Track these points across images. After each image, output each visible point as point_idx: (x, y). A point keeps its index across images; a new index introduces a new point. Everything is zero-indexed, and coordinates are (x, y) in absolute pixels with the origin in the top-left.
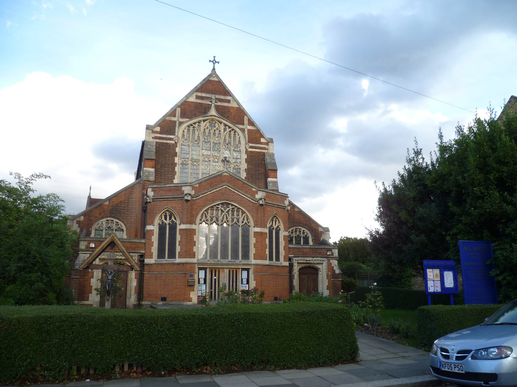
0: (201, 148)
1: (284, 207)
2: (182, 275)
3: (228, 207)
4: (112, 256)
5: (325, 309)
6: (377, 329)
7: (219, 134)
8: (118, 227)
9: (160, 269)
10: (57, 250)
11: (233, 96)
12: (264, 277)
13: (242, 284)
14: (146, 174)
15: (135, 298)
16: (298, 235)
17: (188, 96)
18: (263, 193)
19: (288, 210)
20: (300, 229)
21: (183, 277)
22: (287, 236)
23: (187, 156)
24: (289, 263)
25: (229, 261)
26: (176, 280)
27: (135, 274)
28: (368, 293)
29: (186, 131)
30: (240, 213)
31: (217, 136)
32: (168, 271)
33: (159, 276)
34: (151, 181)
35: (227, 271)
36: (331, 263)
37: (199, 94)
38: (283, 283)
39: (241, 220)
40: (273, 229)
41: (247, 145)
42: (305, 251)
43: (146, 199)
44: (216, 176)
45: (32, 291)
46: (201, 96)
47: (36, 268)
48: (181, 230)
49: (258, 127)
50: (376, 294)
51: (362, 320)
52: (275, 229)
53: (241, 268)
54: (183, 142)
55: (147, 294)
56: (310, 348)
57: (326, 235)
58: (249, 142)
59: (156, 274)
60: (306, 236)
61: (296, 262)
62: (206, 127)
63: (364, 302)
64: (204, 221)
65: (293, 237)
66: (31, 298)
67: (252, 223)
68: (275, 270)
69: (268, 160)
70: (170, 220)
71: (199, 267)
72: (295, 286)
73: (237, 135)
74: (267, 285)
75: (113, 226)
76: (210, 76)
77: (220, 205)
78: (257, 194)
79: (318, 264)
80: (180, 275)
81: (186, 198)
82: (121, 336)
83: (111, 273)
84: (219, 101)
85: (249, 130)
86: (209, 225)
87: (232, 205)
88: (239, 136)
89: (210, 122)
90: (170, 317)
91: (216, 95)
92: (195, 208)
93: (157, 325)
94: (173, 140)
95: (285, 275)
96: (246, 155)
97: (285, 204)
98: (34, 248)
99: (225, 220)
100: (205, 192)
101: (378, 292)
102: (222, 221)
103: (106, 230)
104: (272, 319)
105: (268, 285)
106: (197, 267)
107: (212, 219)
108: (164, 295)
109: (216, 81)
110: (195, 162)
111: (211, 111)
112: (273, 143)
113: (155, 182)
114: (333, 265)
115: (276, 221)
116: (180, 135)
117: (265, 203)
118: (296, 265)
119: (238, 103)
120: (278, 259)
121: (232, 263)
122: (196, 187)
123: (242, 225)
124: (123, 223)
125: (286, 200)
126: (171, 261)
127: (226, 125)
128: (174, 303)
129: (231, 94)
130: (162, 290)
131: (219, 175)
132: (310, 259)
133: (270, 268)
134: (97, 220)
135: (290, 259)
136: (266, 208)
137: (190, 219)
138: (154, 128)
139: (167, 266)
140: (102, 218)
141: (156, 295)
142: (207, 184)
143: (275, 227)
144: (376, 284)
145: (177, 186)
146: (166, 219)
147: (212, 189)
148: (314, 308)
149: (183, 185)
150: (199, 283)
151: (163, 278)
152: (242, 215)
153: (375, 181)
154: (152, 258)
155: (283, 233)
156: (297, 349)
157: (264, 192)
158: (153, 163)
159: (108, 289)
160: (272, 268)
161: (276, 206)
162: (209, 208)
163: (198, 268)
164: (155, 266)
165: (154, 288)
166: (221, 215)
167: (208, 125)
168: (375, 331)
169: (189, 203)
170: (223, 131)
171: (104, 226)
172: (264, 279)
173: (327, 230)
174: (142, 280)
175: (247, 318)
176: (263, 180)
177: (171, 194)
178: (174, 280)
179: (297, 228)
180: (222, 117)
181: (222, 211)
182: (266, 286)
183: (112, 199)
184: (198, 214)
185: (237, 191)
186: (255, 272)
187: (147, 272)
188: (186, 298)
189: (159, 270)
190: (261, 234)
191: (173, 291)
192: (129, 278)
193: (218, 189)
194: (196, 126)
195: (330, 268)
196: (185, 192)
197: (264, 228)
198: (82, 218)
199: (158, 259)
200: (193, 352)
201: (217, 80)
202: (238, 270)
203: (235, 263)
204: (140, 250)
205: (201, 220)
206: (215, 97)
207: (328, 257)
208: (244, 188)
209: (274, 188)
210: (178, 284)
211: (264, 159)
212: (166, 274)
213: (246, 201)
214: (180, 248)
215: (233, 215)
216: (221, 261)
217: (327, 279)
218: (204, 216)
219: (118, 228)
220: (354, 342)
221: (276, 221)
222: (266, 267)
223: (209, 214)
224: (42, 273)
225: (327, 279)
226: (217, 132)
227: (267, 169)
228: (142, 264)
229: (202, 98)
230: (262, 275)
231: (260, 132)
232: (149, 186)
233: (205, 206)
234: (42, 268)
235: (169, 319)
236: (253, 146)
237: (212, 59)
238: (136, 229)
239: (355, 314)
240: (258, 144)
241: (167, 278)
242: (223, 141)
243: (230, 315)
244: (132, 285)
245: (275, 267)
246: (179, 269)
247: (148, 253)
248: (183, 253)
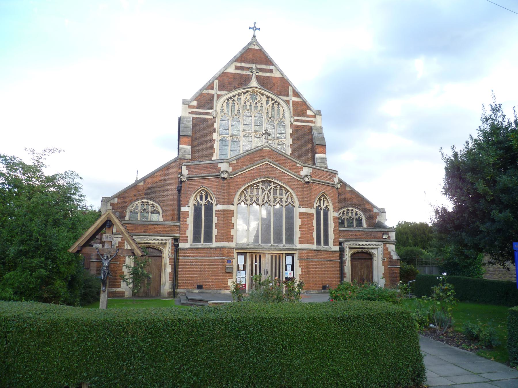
0: (242, 123)
2: (220, 261)
3: (270, 186)
4: (108, 237)
5: (375, 313)
6: (447, 332)
7: (261, 107)
8: (154, 209)
9: (195, 254)
10: (68, 231)
11: (276, 66)
12: (311, 263)
13: (286, 270)
14: (182, 151)
15: (170, 285)
16: (350, 217)
17: (226, 67)
18: (309, 170)
19: (338, 189)
20: (352, 210)
21: (220, 263)
22: (336, 217)
23: (227, 131)
24: (340, 248)
25: (271, 246)
26: (212, 266)
27: (170, 260)
28: (435, 286)
29: (225, 104)
30: (284, 192)
31: (259, 109)
32: (204, 257)
33: (194, 261)
34: (187, 159)
35: (269, 256)
36: (388, 248)
37: (239, 64)
39: (284, 200)
40: (321, 209)
41: (292, 119)
42: (358, 234)
43: (180, 177)
44: (256, 151)
45: (33, 278)
46: (241, 66)
47: (39, 253)
48: (217, 211)
49: (303, 98)
50: (446, 287)
51: (428, 320)
52: (323, 209)
53: (285, 253)
54: (222, 116)
55: (183, 281)
56: (352, 370)
57: (381, 216)
58: (294, 115)
59: (192, 260)
60: (359, 217)
61: (348, 246)
62: (247, 99)
63: (430, 298)
64: (243, 201)
65: (344, 219)
66: (31, 286)
67: (297, 203)
69: (315, 132)
70: (205, 200)
71: (238, 251)
72: (346, 273)
73: (281, 108)
74: (314, 272)
75: (149, 208)
76: (250, 44)
77: (261, 184)
78: (302, 170)
79: (372, 248)
80: (217, 261)
81: (222, 175)
82: (75, 349)
83: (107, 258)
84: (260, 72)
85: (294, 102)
86: (249, 205)
87: (275, 183)
88: (283, 109)
89: (251, 94)
90: (145, 321)
91: (257, 65)
92: (233, 187)
93: (127, 333)
94: (211, 115)
95: (335, 262)
96: (291, 129)
97: (334, 182)
98: (36, 229)
99: (266, 199)
100: (244, 169)
101: (449, 284)
102: (263, 201)
103: (141, 212)
104: (295, 326)
106: (235, 251)
107: (251, 198)
108: (200, 283)
109: (257, 50)
110: (235, 137)
111: (251, 82)
112: (321, 115)
113: (192, 160)
114: (389, 250)
115: (324, 201)
116: (219, 109)
117: (311, 180)
118: (348, 250)
119: (281, 72)
120: (326, 243)
121: (275, 247)
122: (234, 163)
123: (286, 206)
124: (159, 205)
125: (335, 177)
126: (207, 245)
127: (268, 97)
128: (210, 291)
129: (273, 63)
130: (198, 276)
131: (259, 150)
132: (364, 243)
133: (318, 253)
134: (131, 203)
135: (340, 244)
137: (227, 198)
138: (191, 102)
139: (202, 251)
140: (137, 200)
141: (192, 282)
142: (246, 160)
143: (323, 207)
144: (445, 274)
145: (213, 162)
146: (201, 199)
147: (251, 165)
148: (359, 310)
149: (219, 161)
150: (238, 269)
151: (199, 264)
152: (286, 194)
153: (441, 148)
154: (187, 242)
155: (332, 214)
156: (333, 370)
157: (310, 168)
158: (189, 140)
159: (102, 278)
161: (324, 184)
162: (248, 187)
163: (237, 252)
164: (190, 251)
165: (189, 275)
166: (262, 194)
167: (249, 97)
168: (445, 334)
169: (225, 181)
170: (265, 103)
171: (139, 209)
172: (311, 266)
173: (383, 211)
174: (177, 266)
175: (259, 325)
176: (310, 157)
177: (207, 172)
178: (210, 266)
181: (263, 190)
183: (147, 180)
184: (236, 193)
185: (279, 167)
186: (300, 258)
187: (181, 257)
188: (223, 286)
189: (194, 255)
190: (307, 214)
191: (210, 278)
192: (163, 264)
193: (258, 166)
194: (236, 98)
195: (387, 253)
196: (222, 170)
198: (116, 200)
199: (193, 243)
200: (179, 372)
201: (258, 48)
202: (281, 255)
203: (277, 247)
204: (174, 234)
205: (239, 200)
206: (256, 66)
207: (384, 241)
208: (287, 164)
209: (322, 164)
210: (215, 270)
211: (311, 134)
212: (202, 259)
213: (290, 178)
214: (217, 231)
215: (275, 194)
216: (262, 246)
217: (383, 266)
218: (243, 196)
219: (154, 210)
220: (419, 359)
221: (324, 201)
223: (249, 193)
224: (47, 259)
225: (383, 266)
226: (259, 105)
227: (315, 144)
228: (177, 249)
229: (242, 68)
230: (308, 261)
231: (306, 103)
232: (183, 164)
233: (244, 185)
234: (46, 252)
235: (145, 324)
237: (252, 26)
238: (173, 211)
239: (417, 312)
240: (304, 117)
241: (203, 264)
242: (265, 114)
243: (234, 321)
244: (167, 271)
245: (323, 252)
246: (216, 253)
247: (182, 236)
248: (220, 237)
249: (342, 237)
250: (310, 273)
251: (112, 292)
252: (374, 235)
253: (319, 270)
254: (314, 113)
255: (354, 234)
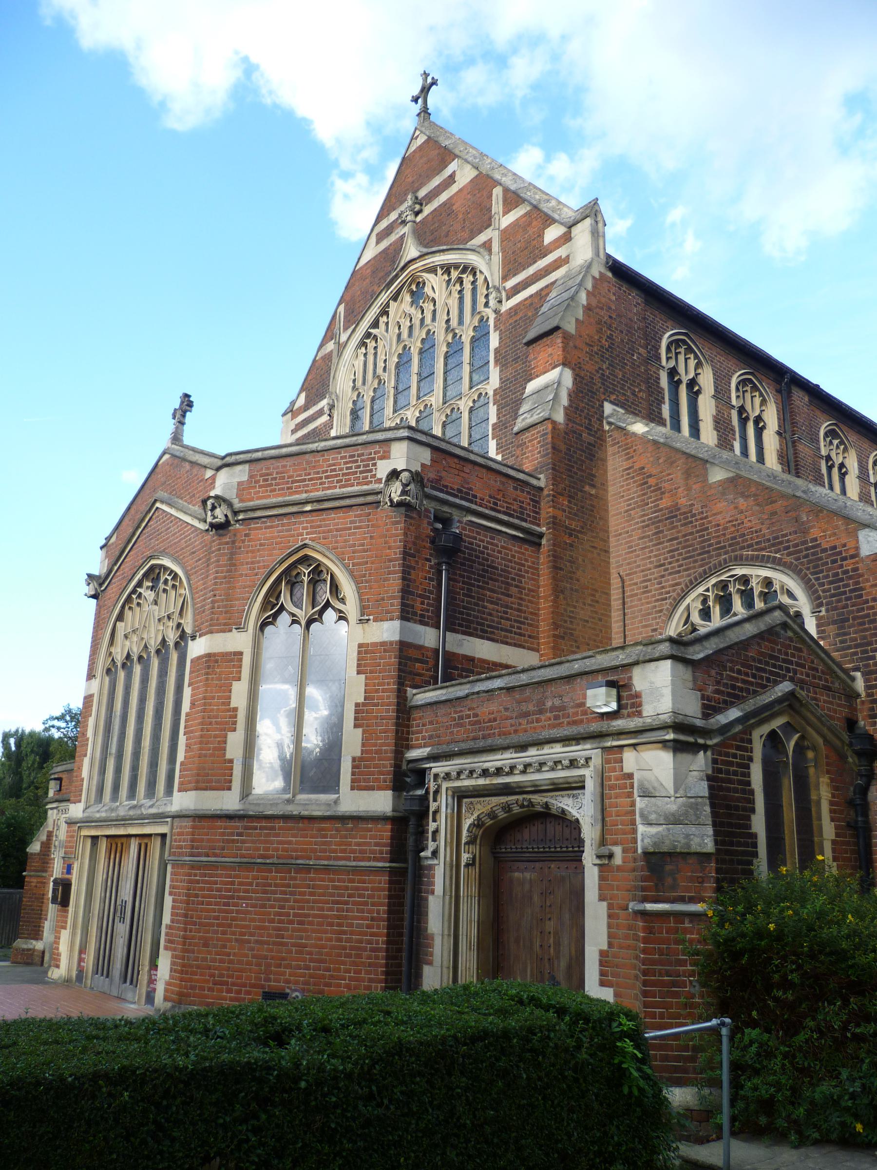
1: (370, 499)
20: (745, 580)
22: (383, 644)
38: (338, 917)
61: (445, 785)
68: (280, 843)
72: (432, 937)
74: (217, 918)
79: (558, 787)
105: (226, 918)
127: (447, 269)
136: (246, 535)
157: (239, 468)
160: (261, 828)
172: (202, 889)
179: (723, 578)
180: (449, 247)
182: (212, 925)
197: (224, 631)
209: (532, 416)
222: (219, 823)
236: (519, 284)
237: (416, 91)
240: (535, 262)
249: (424, 738)
250: (195, 924)
251: (24, 950)
252: (557, 702)
253: (247, 912)
254: (562, 224)
255: (468, 716)
